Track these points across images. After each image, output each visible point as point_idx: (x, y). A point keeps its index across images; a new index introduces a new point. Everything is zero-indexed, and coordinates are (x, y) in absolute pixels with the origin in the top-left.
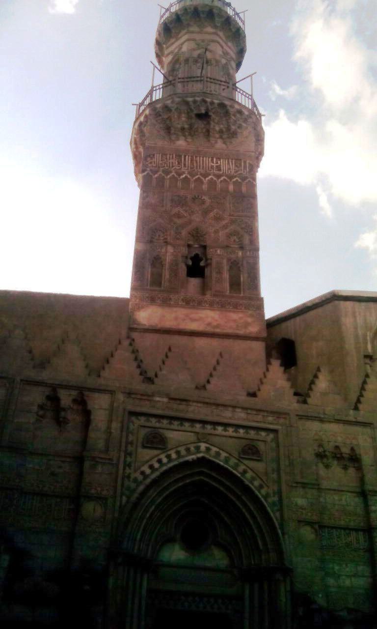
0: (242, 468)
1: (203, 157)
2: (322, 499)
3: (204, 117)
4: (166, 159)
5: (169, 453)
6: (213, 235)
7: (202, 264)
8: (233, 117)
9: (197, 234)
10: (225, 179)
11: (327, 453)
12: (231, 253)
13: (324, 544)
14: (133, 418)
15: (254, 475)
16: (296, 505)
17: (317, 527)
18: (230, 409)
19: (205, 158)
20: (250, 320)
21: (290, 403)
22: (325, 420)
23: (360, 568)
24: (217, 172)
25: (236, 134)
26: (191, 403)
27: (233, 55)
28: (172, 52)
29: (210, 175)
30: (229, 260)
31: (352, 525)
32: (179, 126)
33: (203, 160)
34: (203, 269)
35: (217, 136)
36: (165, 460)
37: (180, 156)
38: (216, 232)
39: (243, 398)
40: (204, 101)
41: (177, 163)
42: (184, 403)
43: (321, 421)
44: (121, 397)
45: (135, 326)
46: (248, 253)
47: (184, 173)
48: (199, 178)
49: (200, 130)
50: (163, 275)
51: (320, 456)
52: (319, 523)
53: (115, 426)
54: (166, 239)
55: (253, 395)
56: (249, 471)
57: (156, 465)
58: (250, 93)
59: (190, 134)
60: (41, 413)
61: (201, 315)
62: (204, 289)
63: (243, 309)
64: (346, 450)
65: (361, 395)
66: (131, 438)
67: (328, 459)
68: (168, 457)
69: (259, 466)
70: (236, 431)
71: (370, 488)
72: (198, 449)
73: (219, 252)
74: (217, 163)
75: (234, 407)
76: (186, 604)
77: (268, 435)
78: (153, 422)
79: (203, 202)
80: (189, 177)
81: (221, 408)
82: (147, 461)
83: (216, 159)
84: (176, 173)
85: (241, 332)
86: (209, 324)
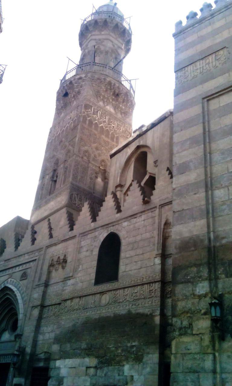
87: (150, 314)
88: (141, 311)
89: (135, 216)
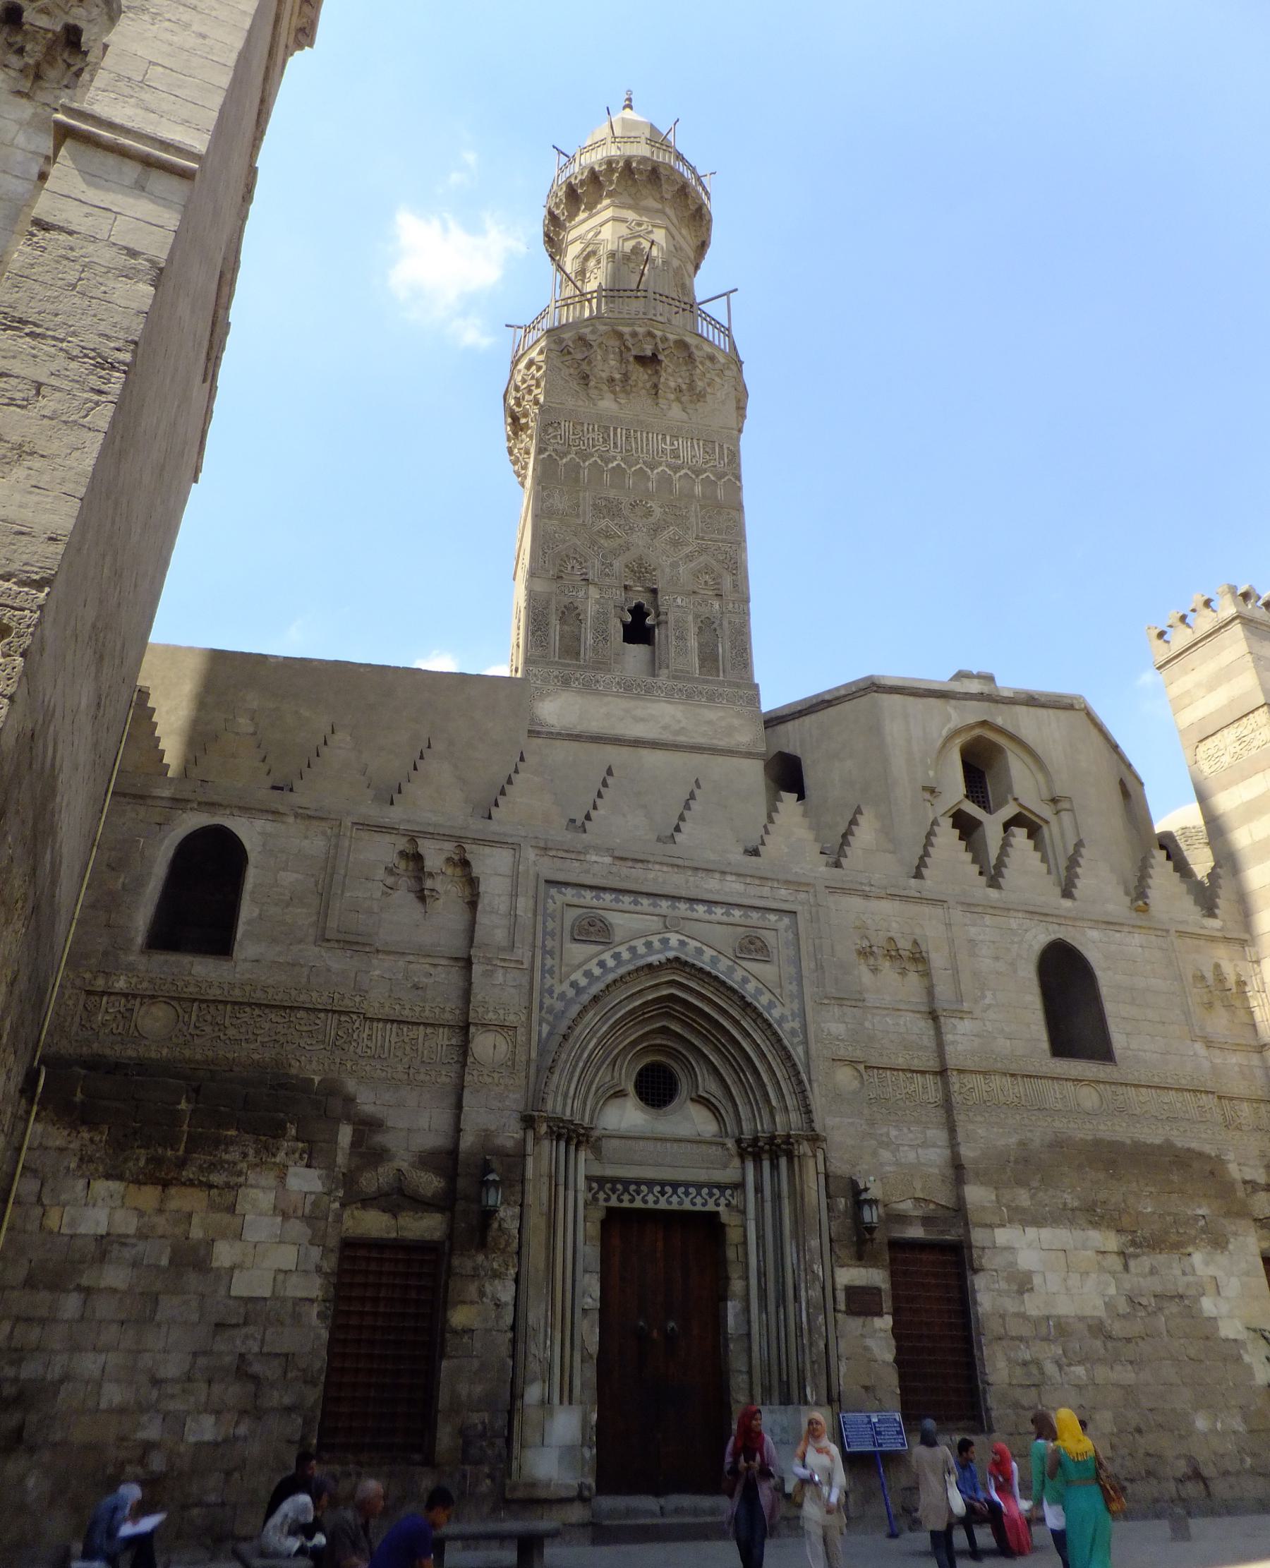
0: (739, 974)
1: (647, 433)
2: (867, 1024)
3: (650, 361)
4: (583, 431)
5: (617, 950)
6: (667, 570)
7: (649, 621)
8: (700, 367)
9: (640, 570)
10: (686, 474)
11: (875, 949)
12: (699, 604)
13: (872, 1096)
14: (553, 891)
15: (761, 986)
16: (829, 1034)
17: (861, 1067)
18: (717, 876)
19: (650, 435)
20: (736, 722)
21: (814, 866)
22: (871, 894)
23: (930, 1133)
24: (673, 460)
25: (704, 396)
26: (650, 866)
27: (692, 255)
28: (580, 238)
29: (660, 464)
30: (697, 616)
31: (916, 1064)
32: (604, 375)
33: (647, 437)
34: (653, 627)
35: (672, 397)
36: (611, 963)
37: (607, 428)
38: (674, 565)
39: (736, 856)
40: (650, 334)
41: (601, 440)
42: (640, 865)
43: (867, 896)
44: (531, 854)
45: (538, 728)
46: (731, 605)
47: (615, 458)
48: (641, 468)
49: (641, 385)
50: (583, 636)
51: (865, 953)
52: (865, 1062)
53: (524, 904)
54: (586, 574)
55: (755, 852)
56: (751, 978)
57: (597, 971)
58: (727, 326)
59: (624, 391)
60: (390, 881)
62: (654, 666)
63: (725, 702)
64: (904, 944)
65: (926, 854)
66: (550, 925)
67: (876, 959)
68: (616, 956)
69: (767, 971)
70: (728, 914)
71: (946, 1006)
72: (665, 942)
73: (679, 600)
75: (723, 873)
76: (651, 1198)
77: (780, 919)
78: (588, 897)
79: (649, 513)
80: (623, 465)
81: (700, 874)
82: (580, 966)
83: (671, 436)
84: (601, 457)
85: (722, 743)
86: (665, 728)
87: (1216, 1156)
88: (1194, 1145)
89: (1117, 928)
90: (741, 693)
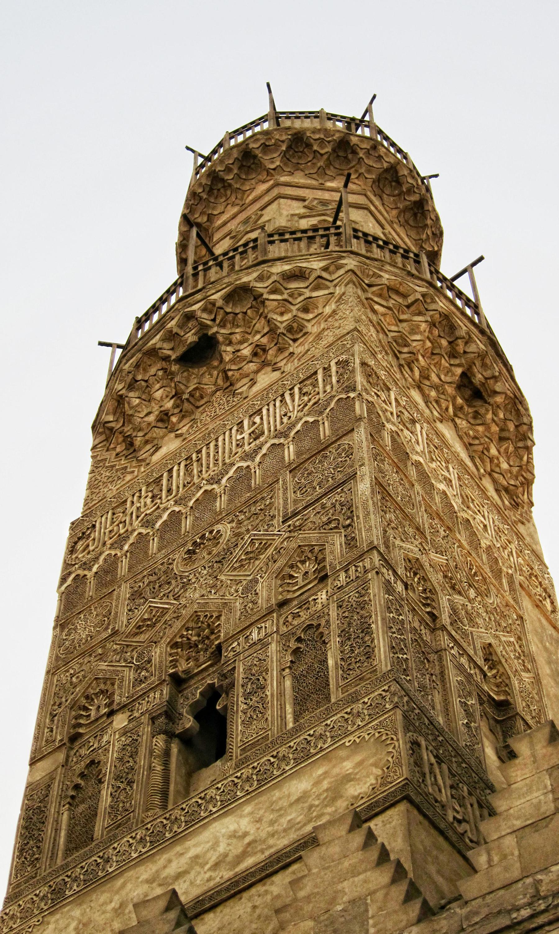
19: (220, 439)
35: (252, 367)
40: (189, 317)
46: (343, 575)
61: (192, 853)
74: (254, 423)
90: (358, 707)
